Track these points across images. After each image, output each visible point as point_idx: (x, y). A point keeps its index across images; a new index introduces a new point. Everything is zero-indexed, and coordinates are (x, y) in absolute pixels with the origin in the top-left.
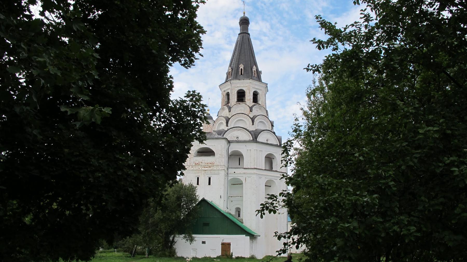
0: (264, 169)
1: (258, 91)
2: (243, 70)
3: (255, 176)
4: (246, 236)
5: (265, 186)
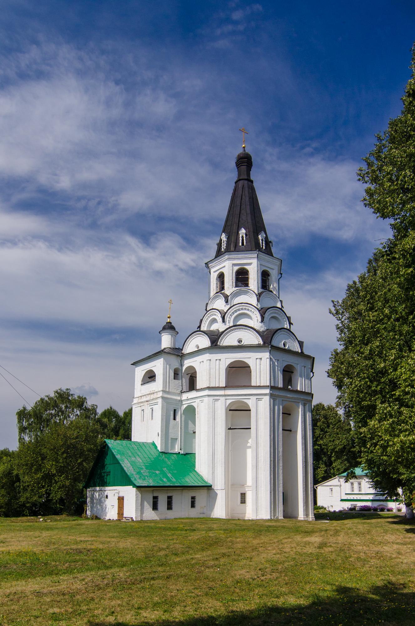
0: (224, 386)
1: (246, 267)
2: (245, 238)
3: (206, 399)
4: (133, 487)
5: (250, 410)
